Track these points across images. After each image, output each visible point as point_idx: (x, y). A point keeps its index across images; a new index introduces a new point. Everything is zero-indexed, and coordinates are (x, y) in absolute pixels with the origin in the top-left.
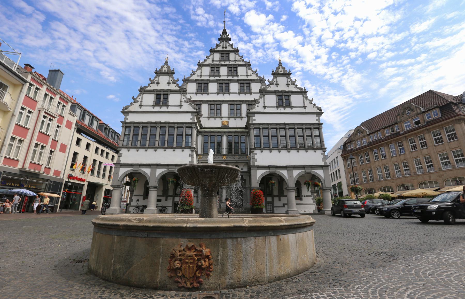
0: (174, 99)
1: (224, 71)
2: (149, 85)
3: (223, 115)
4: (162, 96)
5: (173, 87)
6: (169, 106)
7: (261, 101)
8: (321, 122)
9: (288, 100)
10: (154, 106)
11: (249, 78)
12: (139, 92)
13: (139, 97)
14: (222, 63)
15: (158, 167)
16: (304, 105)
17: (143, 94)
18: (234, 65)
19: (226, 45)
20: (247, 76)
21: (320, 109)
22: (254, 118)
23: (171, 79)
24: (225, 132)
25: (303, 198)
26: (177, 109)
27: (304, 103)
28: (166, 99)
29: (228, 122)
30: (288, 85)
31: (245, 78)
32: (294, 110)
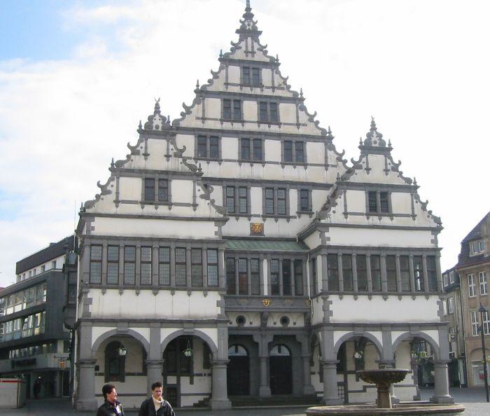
0: (181, 190)
1: (250, 109)
2: (128, 156)
5: (175, 164)
6: (172, 204)
7: (340, 201)
8: (439, 246)
10: (143, 203)
11: (302, 131)
12: (109, 174)
13: (112, 183)
14: (247, 90)
15: (164, 325)
18: (270, 97)
19: (253, 47)
20: (298, 125)
21: (437, 220)
22: (327, 235)
23: (171, 147)
24: (265, 254)
26: (188, 212)
27: (413, 208)
28: (165, 190)
29: (262, 226)
30: (386, 171)
31: (292, 130)
32: (396, 222)
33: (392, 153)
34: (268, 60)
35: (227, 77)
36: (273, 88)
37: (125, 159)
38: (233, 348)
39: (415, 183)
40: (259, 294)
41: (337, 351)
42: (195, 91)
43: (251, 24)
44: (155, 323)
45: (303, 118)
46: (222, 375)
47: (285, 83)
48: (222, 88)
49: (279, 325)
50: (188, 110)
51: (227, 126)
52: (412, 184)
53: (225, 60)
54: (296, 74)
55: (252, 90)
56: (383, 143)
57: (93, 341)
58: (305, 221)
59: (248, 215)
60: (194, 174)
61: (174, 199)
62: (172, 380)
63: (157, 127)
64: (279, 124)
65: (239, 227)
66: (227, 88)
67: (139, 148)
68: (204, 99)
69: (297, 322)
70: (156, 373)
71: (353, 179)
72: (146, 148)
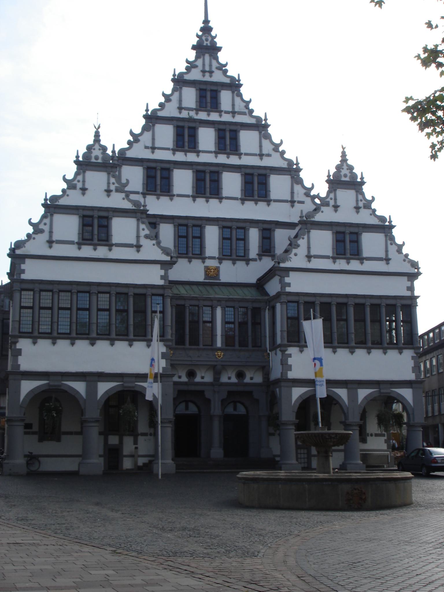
0: (123, 229)
1: (207, 138)
2: (64, 191)
3: (208, 253)
4: (96, 222)
5: (117, 201)
8: (416, 294)
9: (356, 242)
10: (79, 245)
11: (266, 162)
14: (203, 116)
16: (387, 254)
17: (52, 215)
19: (211, 65)
20: (261, 156)
21: (415, 265)
22: (287, 280)
23: (113, 180)
25: (369, 439)
26: (130, 254)
27: (387, 251)
29: (217, 269)
30: (357, 208)
32: (368, 266)
33: (365, 188)
34: (228, 81)
35: (180, 101)
36: (234, 113)
37: (60, 193)
38: (182, 406)
39: (390, 222)
40: (212, 345)
41: (296, 409)
42: (145, 117)
43: (210, 39)
44: (92, 378)
45: (267, 148)
46: (165, 435)
47: (247, 107)
48: (175, 114)
49: (234, 380)
50: (136, 138)
51: (180, 157)
52: (387, 224)
53: (179, 81)
54: (260, 96)
55: (209, 115)
56: (355, 176)
57: (22, 398)
58: (267, 263)
59: (201, 256)
60: (139, 213)
61: (115, 239)
62: (113, 440)
63: (97, 158)
64: (240, 155)
65: (190, 271)
66: (180, 113)
67: (75, 182)
68: (154, 125)
69: (253, 377)
70: (94, 431)
71: (319, 217)
72: (84, 181)
